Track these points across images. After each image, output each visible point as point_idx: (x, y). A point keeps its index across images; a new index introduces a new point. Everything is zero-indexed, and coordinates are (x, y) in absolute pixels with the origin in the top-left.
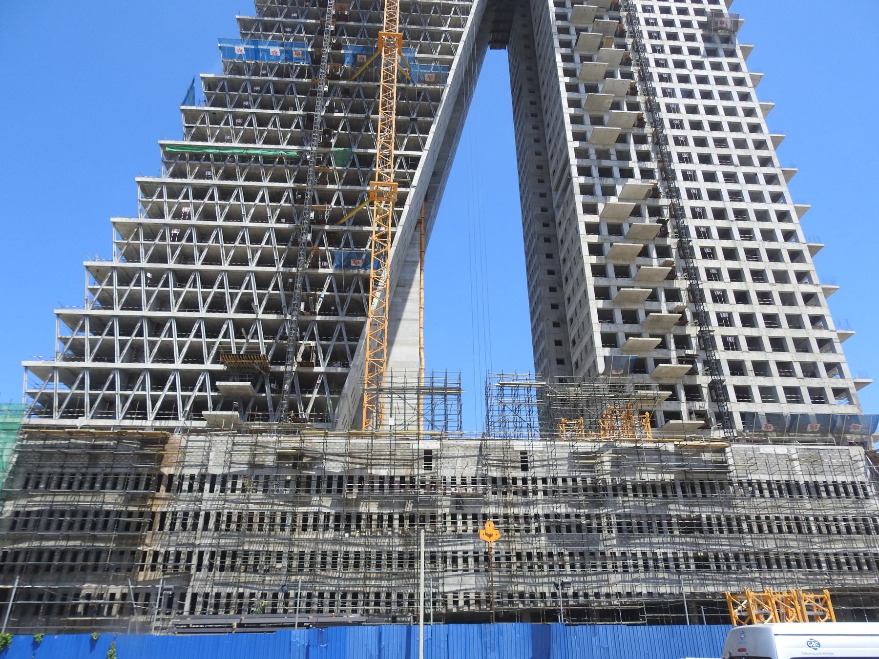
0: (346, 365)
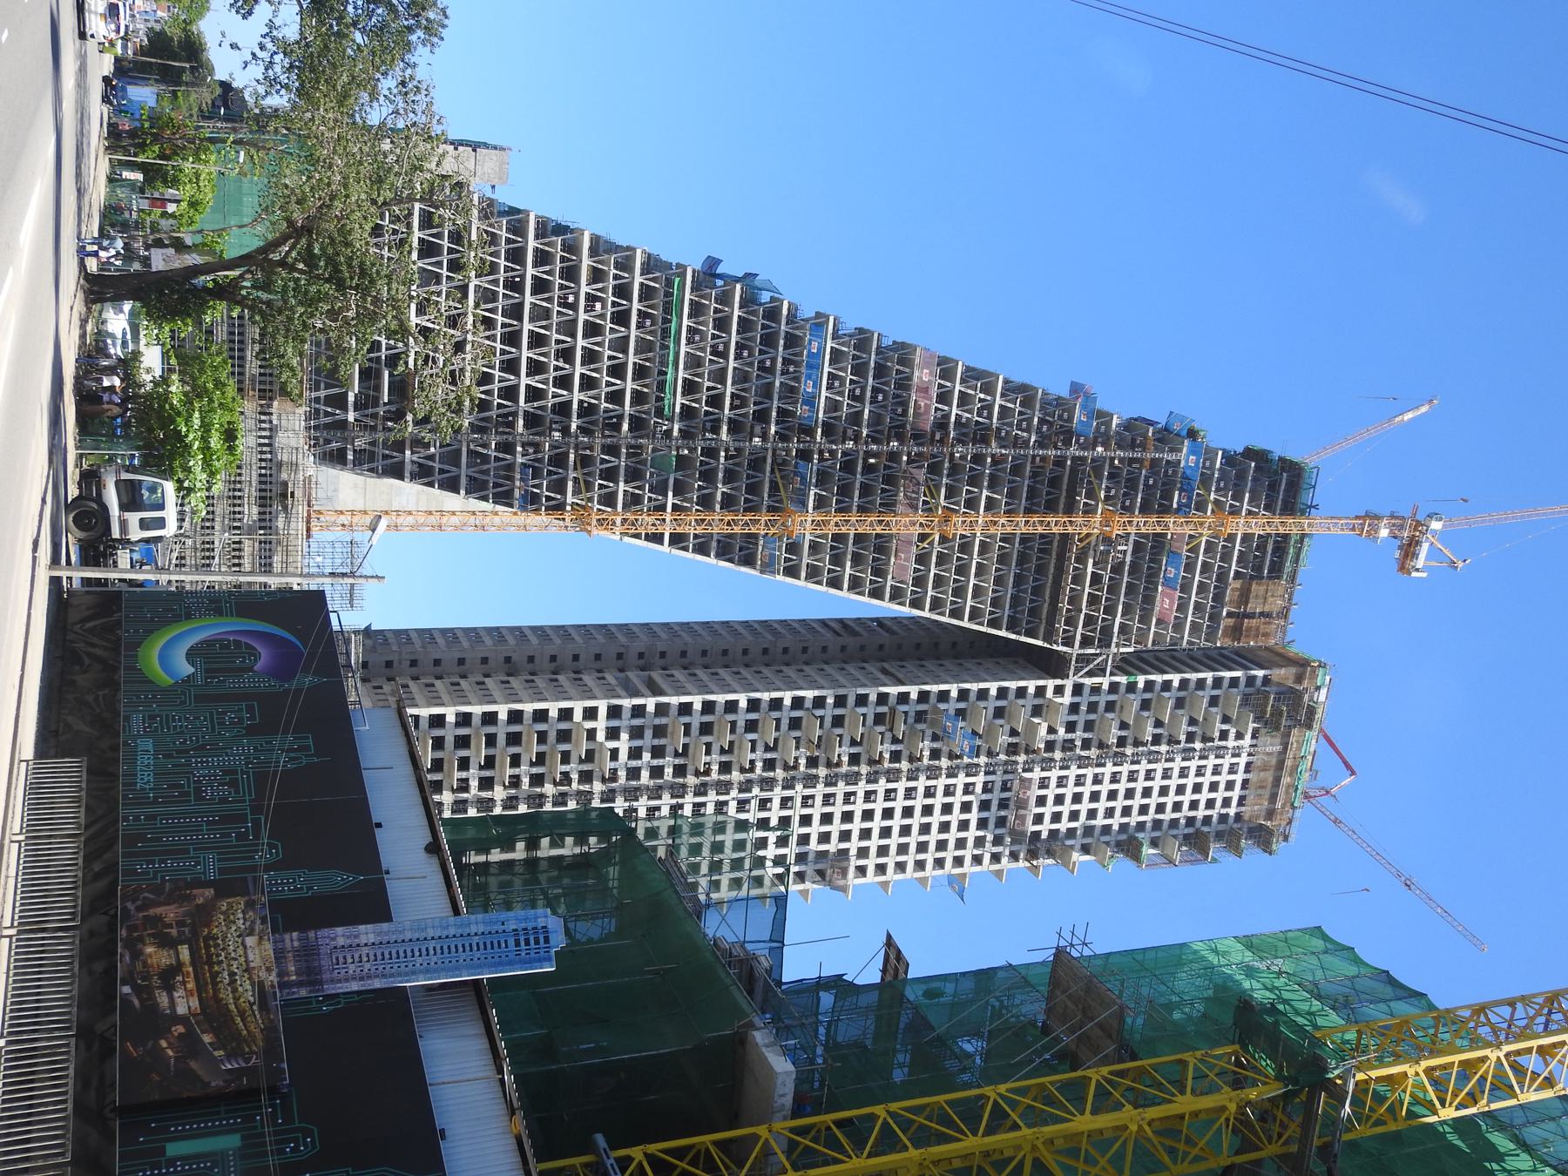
0: (413, 477)
